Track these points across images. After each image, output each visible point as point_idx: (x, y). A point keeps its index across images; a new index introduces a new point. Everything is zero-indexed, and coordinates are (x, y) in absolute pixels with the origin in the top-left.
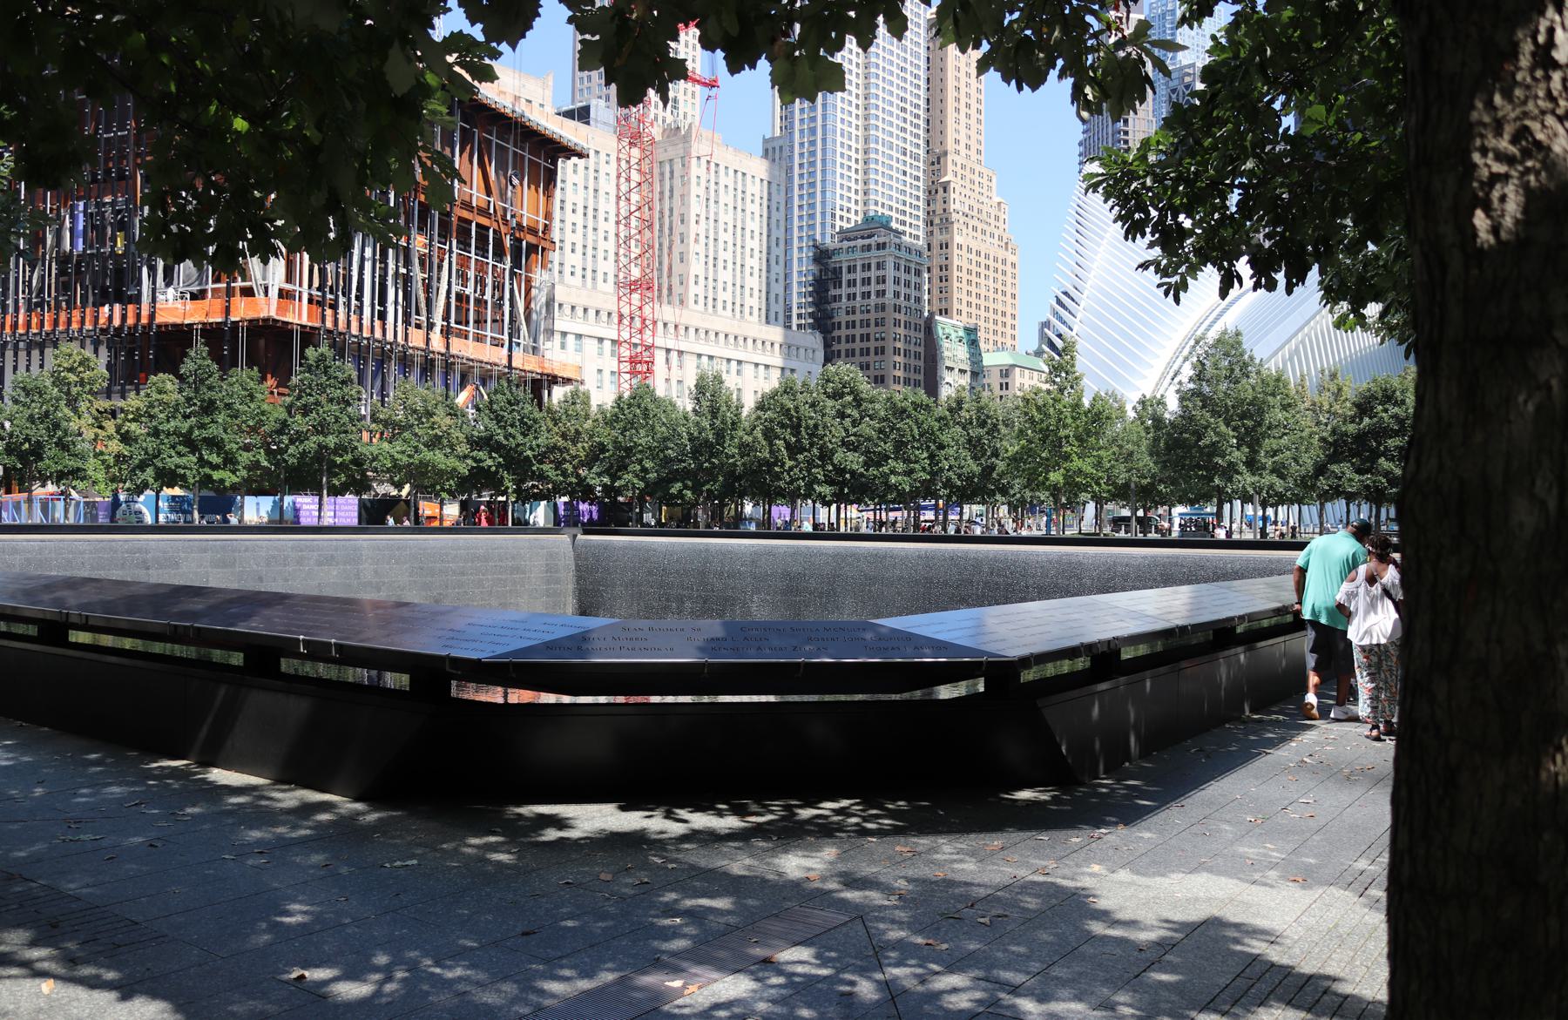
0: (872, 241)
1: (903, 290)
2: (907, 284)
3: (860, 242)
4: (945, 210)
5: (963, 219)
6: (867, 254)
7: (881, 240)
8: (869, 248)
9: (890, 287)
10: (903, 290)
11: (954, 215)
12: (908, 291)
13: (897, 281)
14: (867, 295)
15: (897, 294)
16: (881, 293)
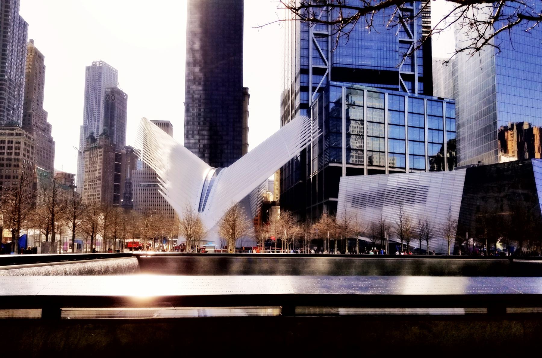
0: (14, 132)
1: (27, 154)
2: (28, 152)
3: (7, 131)
4: (29, 124)
5: (36, 128)
6: (11, 137)
7: (19, 132)
8: (12, 134)
9: (22, 152)
10: (27, 154)
11: (33, 126)
12: (28, 154)
13: (25, 150)
14: (9, 154)
15: (24, 155)
16: (18, 154)
